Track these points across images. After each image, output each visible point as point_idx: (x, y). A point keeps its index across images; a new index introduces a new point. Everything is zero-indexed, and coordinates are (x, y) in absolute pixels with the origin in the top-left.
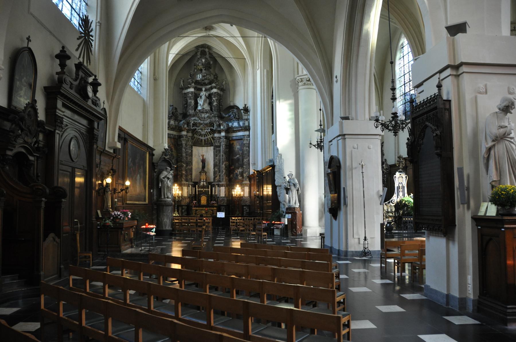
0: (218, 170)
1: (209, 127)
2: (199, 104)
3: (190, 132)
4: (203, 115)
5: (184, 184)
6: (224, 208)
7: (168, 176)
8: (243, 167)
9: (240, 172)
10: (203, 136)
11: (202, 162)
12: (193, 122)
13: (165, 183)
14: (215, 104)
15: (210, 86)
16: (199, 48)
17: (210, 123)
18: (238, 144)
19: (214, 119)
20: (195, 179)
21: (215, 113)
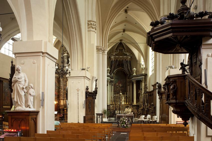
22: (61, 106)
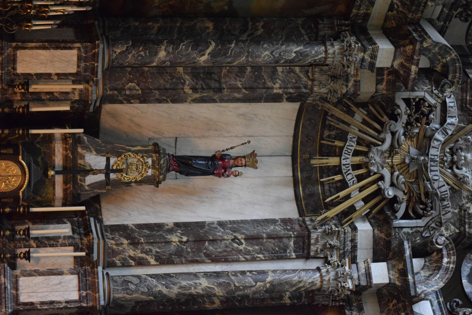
0: (172, 248)
1: (409, 193)
3: (382, 87)
5: (95, 57)
10: (357, 160)
11: (213, 158)
12: (433, 101)
17: (427, 194)
19: (449, 215)
20: (113, 115)
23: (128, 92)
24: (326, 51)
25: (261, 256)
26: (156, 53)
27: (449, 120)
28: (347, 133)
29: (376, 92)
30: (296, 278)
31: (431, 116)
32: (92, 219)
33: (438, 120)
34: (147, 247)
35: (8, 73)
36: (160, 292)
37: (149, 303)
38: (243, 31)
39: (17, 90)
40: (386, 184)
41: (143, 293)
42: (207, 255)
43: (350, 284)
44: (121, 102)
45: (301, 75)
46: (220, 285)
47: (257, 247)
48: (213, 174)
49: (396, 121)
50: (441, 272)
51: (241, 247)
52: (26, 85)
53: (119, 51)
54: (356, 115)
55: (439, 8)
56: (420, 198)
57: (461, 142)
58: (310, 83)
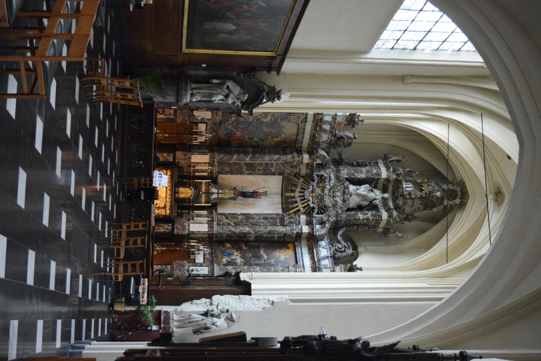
0: (239, 220)
1: (318, 205)
2: (358, 187)
3: (308, 170)
4: (339, 194)
5: (214, 157)
6: (168, 229)
7: (231, 95)
8: (245, 265)
9: (235, 260)
10: (301, 194)
11: (253, 193)
12: (326, 176)
13: (219, 91)
14: (360, 216)
15: (392, 207)
16: (460, 187)
17: (325, 206)
18: (288, 257)
20: (222, 179)
21: (344, 216)
22: (186, 155)
23: (225, 170)
24: (287, 157)
25: (268, 224)
26: (233, 157)
27: (331, 182)
28: (297, 185)
29: (307, 172)
30: (277, 229)
31: (326, 180)
32: (214, 211)
33: (328, 182)
34: (231, 219)
35: (189, 162)
36: (233, 231)
37: (231, 236)
38: (262, 152)
39: (191, 168)
40: (310, 203)
41: (228, 231)
42: (250, 223)
43: (295, 232)
44: (224, 174)
45: (281, 166)
46: (252, 230)
47: (267, 221)
48: (252, 197)
49: (314, 182)
50: (325, 228)
51: (262, 221)
52: (194, 167)
53: (222, 156)
54: (300, 180)
55: (325, 145)
56: (322, 208)
57: (336, 189)
58: (284, 168)
